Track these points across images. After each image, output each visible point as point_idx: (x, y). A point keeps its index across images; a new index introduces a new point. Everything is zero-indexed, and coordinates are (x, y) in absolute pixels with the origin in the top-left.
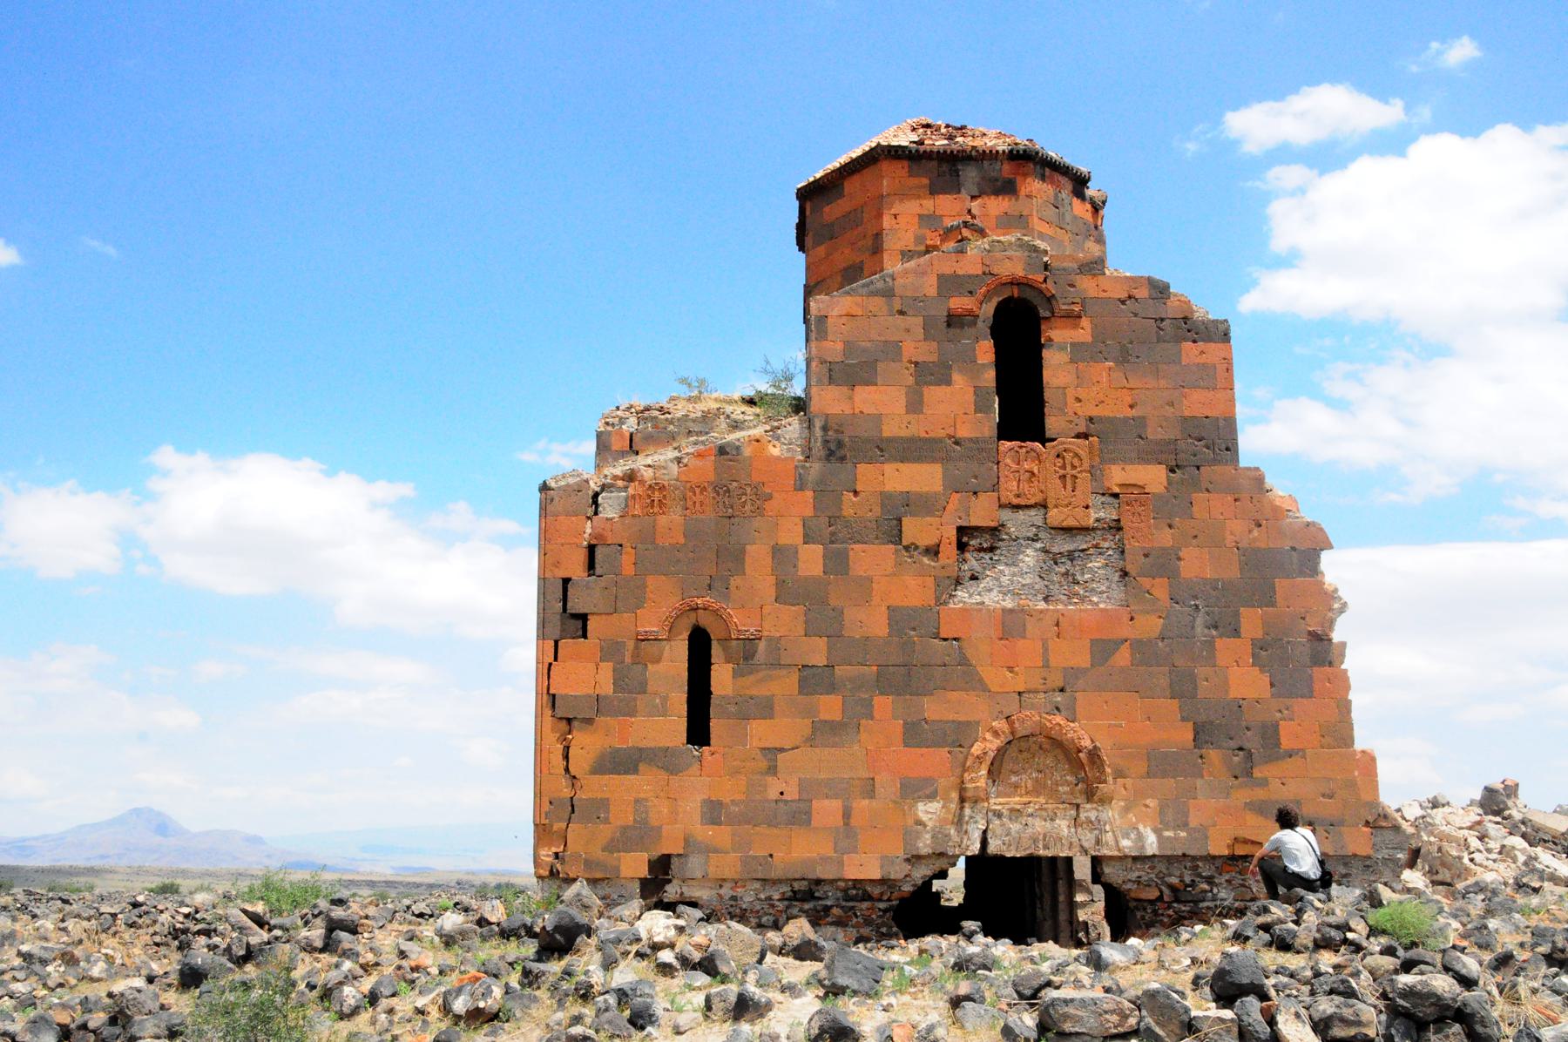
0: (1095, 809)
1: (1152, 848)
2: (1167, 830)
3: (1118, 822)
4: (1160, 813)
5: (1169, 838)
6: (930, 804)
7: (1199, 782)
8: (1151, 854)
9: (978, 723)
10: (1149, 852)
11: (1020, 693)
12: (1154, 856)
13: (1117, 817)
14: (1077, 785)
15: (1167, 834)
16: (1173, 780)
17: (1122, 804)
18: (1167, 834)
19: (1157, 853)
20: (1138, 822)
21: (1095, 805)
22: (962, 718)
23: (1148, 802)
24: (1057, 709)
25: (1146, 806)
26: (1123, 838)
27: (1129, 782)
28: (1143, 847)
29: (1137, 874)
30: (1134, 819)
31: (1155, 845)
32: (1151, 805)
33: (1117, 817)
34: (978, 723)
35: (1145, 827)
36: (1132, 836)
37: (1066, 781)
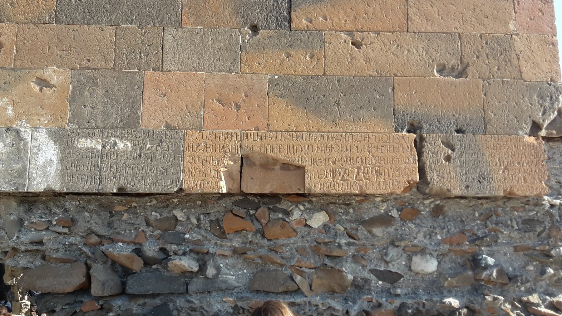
1: (46, 173)
2: (88, 136)
4: (73, 99)
5: (90, 150)
7: (170, 35)
15: (85, 143)
16: (110, 30)
18: (85, 143)
19: (57, 188)
20: (17, 117)
25: (43, 83)
28: (22, 173)
29: (33, 235)
30: (10, 111)
31: (53, 170)
32: (54, 80)
35: (35, 128)
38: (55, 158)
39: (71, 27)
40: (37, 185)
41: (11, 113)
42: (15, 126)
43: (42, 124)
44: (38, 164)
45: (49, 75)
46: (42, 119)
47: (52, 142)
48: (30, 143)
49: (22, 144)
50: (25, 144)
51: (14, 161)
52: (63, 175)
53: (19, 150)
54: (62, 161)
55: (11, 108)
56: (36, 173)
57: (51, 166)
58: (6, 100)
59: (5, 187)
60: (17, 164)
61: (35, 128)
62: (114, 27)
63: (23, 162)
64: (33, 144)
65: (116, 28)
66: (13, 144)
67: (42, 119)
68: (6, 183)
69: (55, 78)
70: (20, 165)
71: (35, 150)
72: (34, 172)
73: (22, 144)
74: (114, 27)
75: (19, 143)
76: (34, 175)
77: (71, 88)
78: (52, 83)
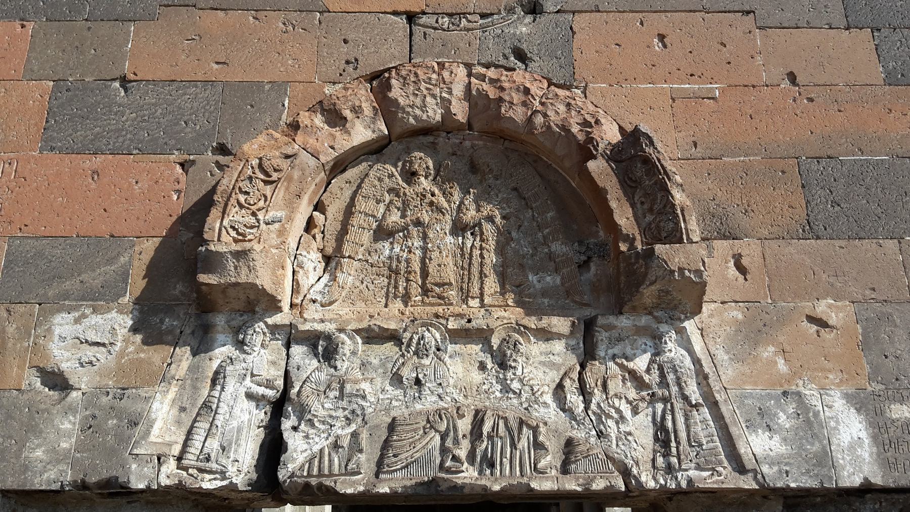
0: (640, 331)
1: (856, 460)
3: (728, 372)
4: (865, 345)
6: (96, 319)
8: (856, 481)
9: (279, 87)
10: (851, 478)
11: (411, 17)
12: (866, 490)
13: (722, 356)
14: (584, 266)
17: (736, 313)
19: (878, 480)
20: (795, 374)
21: (644, 320)
22: (236, 75)
23: (822, 308)
24: (521, 56)
26: (751, 426)
27: (750, 249)
28: (825, 459)
30: (781, 365)
31: (866, 452)
32: (833, 320)
33: (722, 356)
34: (279, 87)
35: (823, 389)
36: (783, 420)
37: (551, 257)
38: (864, 435)
39: (838, 243)
40: (849, 477)
41: (785, 367)
42: (794, 387)
43: (834, 384)
44: (842, 444)
45: (823, 312)
46: (831, 377)
47: (853, 410)
48: (822, 412)
49: (811, 414)
50: (816, 414)
51: (807, 441)
52: (886, 464)
53: (808, 422)
54: (875, 438)
55: (783, 361)
56: (843, 459)
57: (861, 447)
58: (771, 349)
59: (803, 481)
60: (812, 444)
61: (823, 389)
62: (896, 241)
63: (820, 442)
64: (827, 414)
65: (900, 243)
66: (799, 415)
67: (831, 377)
68: (803, 474)
69: (833, 315)
70: (816, 447)
71: (833, 424)
72: (839, 456)
73: (811, 414)
74: (896, 241)
75: (807, 414)
76: (841, 462)
77: (860, 331)
78: (830, 323)
